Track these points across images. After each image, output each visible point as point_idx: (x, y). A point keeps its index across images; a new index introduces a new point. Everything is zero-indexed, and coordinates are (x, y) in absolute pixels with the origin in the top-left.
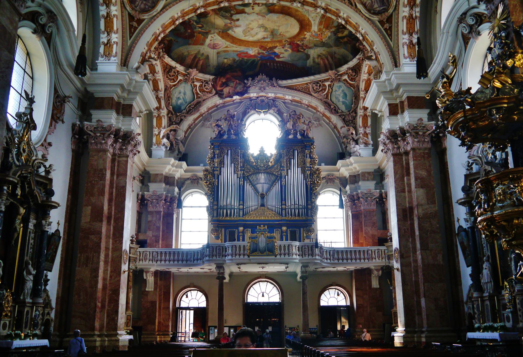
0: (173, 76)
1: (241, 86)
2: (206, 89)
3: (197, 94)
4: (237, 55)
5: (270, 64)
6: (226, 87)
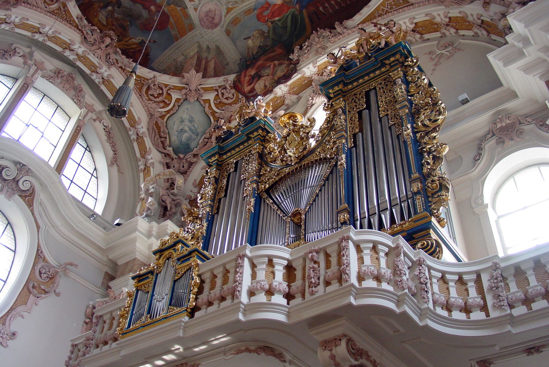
0: (160, 95)
1: (283, 67)
2: (227, 98)
3: (214, 113)
4: (259, 17)
5: (325, 8)
6: (258, 80)
